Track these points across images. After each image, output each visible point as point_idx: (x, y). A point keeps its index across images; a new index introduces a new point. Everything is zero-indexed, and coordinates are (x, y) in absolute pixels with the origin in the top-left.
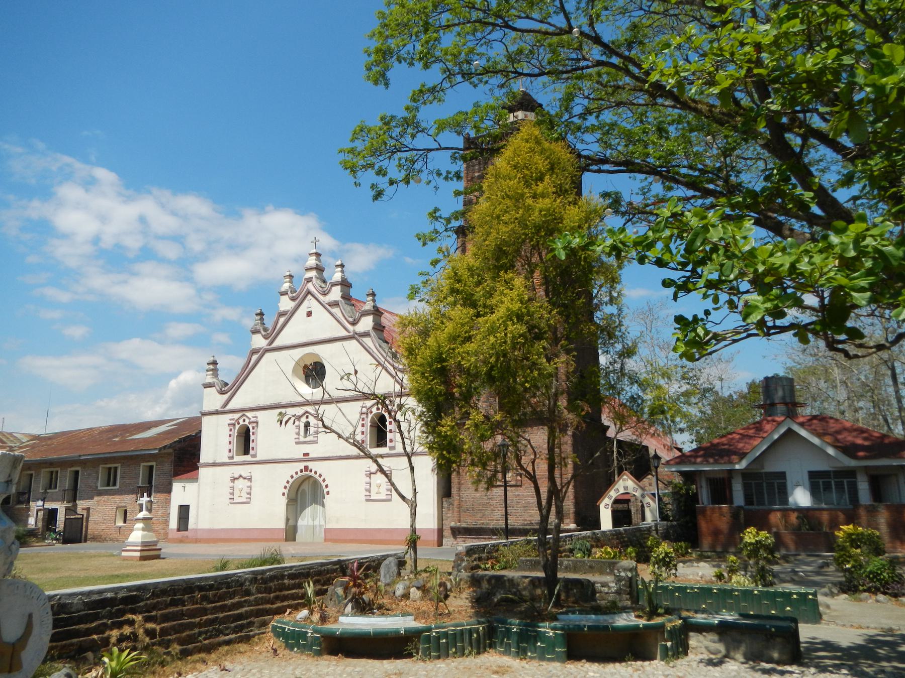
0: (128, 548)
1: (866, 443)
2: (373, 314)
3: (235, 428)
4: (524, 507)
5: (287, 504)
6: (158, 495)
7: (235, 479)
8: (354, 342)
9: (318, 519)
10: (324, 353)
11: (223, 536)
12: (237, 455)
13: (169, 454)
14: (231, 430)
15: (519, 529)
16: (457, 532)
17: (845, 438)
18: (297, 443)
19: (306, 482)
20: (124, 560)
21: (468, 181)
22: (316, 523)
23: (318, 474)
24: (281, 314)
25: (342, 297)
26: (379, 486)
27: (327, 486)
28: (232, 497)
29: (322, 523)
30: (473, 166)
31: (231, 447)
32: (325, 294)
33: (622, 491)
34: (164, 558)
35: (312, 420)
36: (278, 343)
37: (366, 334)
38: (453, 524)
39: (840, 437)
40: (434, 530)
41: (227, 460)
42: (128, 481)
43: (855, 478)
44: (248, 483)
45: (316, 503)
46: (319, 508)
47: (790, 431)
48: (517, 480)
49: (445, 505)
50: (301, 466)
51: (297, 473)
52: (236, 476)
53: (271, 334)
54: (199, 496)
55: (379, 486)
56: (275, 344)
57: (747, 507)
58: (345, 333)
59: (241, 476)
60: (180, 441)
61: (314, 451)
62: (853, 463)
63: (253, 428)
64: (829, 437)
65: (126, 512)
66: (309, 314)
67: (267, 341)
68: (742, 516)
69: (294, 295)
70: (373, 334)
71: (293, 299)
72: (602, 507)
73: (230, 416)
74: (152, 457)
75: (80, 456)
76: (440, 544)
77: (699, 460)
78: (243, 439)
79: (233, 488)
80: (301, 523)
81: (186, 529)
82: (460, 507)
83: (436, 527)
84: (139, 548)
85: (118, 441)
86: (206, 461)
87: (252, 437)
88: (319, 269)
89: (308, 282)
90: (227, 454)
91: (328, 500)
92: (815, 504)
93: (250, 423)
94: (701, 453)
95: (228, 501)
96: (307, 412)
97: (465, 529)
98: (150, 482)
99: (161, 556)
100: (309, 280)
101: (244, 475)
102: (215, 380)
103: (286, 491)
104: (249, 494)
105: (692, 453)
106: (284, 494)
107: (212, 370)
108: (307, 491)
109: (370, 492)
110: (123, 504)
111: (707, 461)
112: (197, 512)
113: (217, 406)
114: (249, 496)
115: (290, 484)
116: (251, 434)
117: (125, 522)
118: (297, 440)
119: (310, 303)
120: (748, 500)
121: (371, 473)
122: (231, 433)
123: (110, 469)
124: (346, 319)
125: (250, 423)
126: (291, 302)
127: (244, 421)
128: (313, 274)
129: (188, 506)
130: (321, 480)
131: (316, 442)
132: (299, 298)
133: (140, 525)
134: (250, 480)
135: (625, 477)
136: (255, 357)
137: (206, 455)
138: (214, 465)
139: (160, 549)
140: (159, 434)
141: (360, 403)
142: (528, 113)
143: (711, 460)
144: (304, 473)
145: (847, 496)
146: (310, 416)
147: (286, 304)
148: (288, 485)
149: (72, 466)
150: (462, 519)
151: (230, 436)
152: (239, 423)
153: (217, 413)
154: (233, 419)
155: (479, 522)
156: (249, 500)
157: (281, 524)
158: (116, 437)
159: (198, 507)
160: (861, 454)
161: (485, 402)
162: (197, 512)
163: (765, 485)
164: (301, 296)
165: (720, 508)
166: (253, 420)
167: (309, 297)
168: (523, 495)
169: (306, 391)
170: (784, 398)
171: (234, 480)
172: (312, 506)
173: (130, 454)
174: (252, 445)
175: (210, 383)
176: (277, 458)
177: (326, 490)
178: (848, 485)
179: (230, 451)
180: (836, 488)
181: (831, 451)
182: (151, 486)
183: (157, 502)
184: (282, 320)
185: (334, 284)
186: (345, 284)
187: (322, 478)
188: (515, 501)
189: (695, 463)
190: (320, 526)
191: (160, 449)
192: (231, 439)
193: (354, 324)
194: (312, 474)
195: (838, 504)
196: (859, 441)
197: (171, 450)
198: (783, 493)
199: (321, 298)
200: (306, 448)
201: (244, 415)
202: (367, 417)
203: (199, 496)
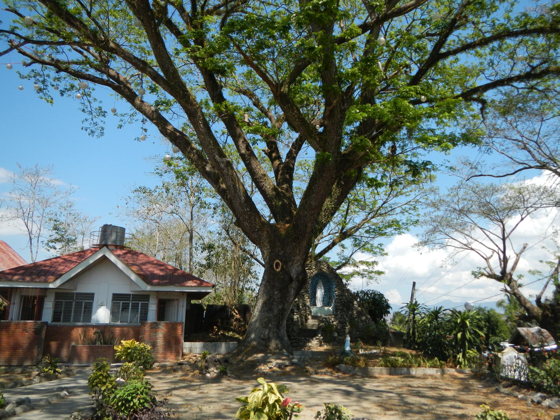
1: (161, 274)
17: (148, 268)
39: (144, 267)
43: (148, 301)
47: (104, 258)
57: (53, 323)
62: (149, 288)
64: (136, 267)
68: (44, 332)
77: (16, 277)
92: (112, 321)
94: (21, 272)
105: (13, 271)
111: (24, 279)
120: (56, 317)
143: (28, 279)
145: (139, 315)
160: (156, 281)
163: (74, 303)
165: (25, 324)
170: (115, 241)
178: (141, 306)
180: (132, 309)
181: (133, 277)
189: (11, 280)
195: (130, 322)
196: (157, 272)
198: (89, 310)
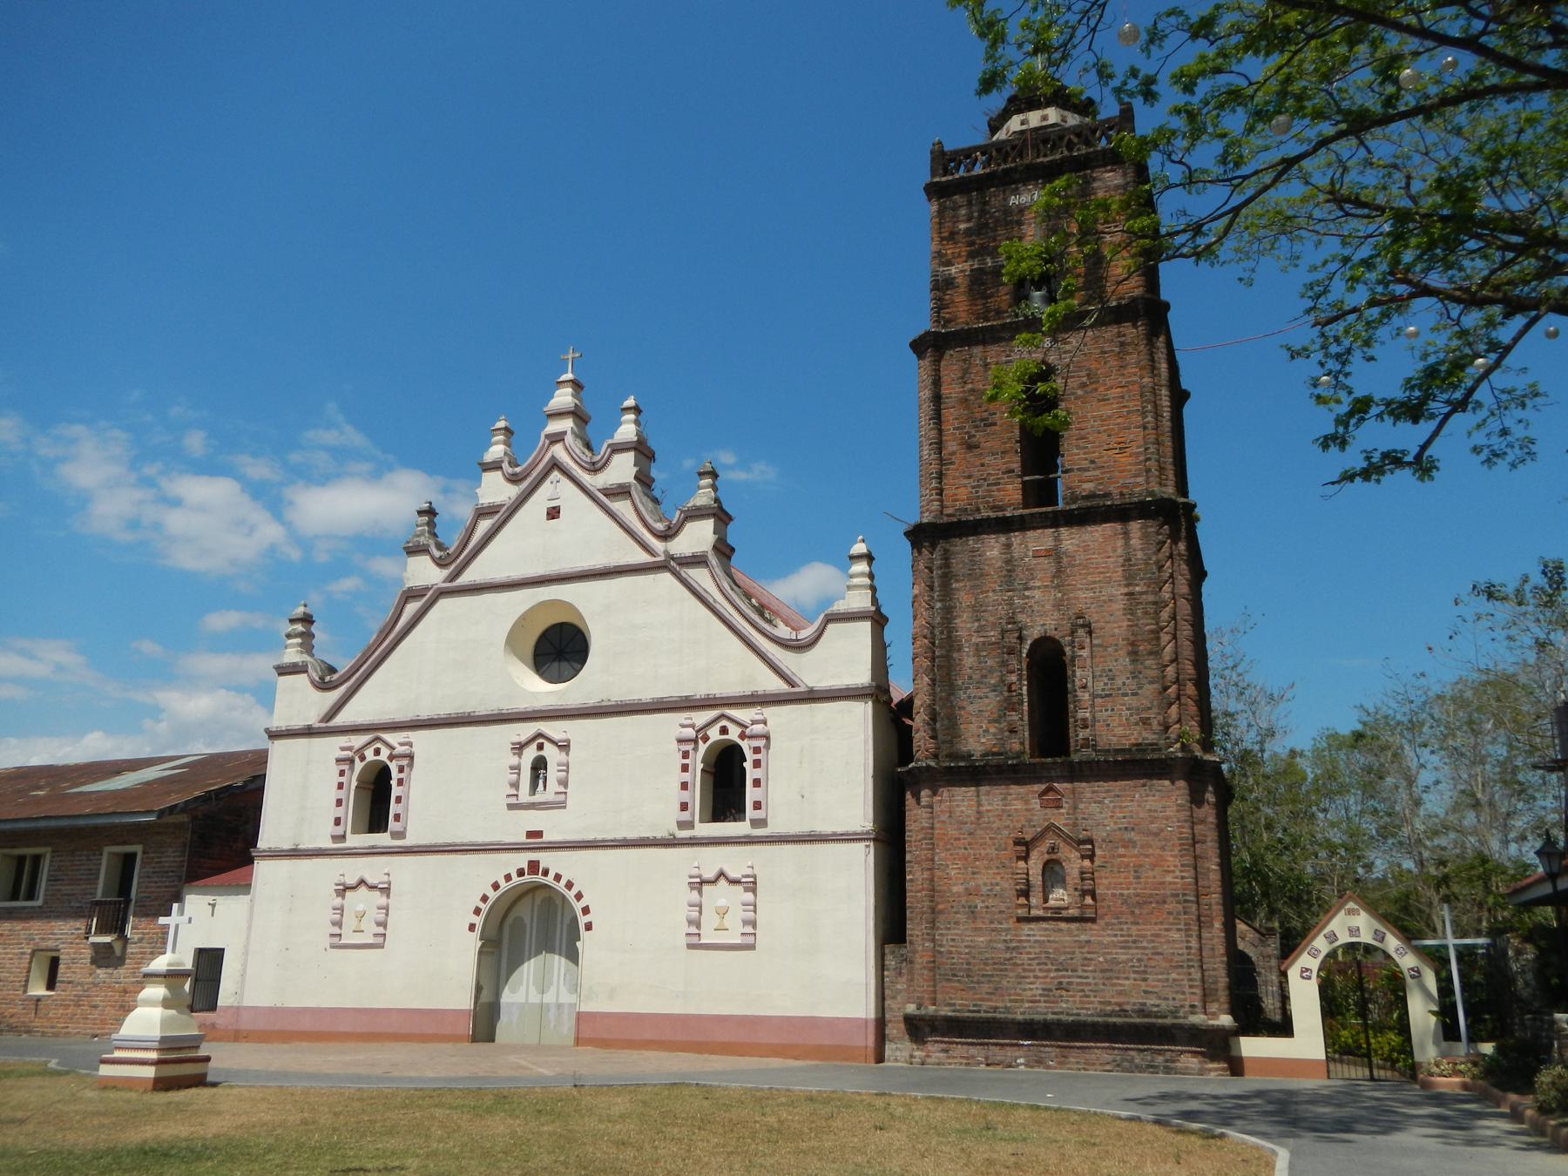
0: (118, 1054)
2: (714, 515)
3: (352, 769)
4: (1103, 971)
5: (480, 953)
6: (144, 922)
7: (347, 888)
8: (666, 577)
9: (553, 989)
10: (587, 602)
11: (307, 1024)
12: (354, 832)
13: (179, 827)
14: (342, 773)
15: (1094, 1025)
16: (918, 1029)
18: (511, 807)
19: (529, 898)
20: (105, 1088)
21: (942, 239)
22: (549, 998)
23: (563, 882)
24: (483, 513)
25: (636, 478)
26: (723, 912)
27: (586, 910)
28: (336, 930)
29: (567, 998)
30: (956, 208)
31: (340, 812)
32: (595, 469)
33: (1344, 938)
34: (214, 1085)
35: (550, 752)
36: (468, 577)
37: (698, 561)
38: (911, 1008)
40: (866, 1021)
41: (328, 844)
42: (67, 889)
44: (378, 898)
45: (551, 950)
46: (558, 962)
48: (1083, 907)
49: (891, 962)
50: (522, 860)
51: (508, 878)
52: (351, 880)
53: (455, 559)
54: (249, 928)
55: (723, 912)
56: (466, 578)
58: (642, 557)
59: (362, 882)
60: (207, 798)
61: (555, 826)
63: (401, 770)
65: (54, 963)
66: (554, 513)
67: (446, 572)
69: (518, 470)
70: (713, 560)
71: (514, 479)
72: (1293, 974)
73: (343, 740)
74: (137, 832)
76: (880, 1058)
78: (368, 796)
79: (341, 909)
80: (507, 997)
81: (212, 1007)
82: (933, 966)
83: (872, 1015)
84: (153, 1055)
85: (44, 797)
86: (273, 845)
87: (396, 791)
88: (578, 415)
89: (553, 443)
90: (330, 828)
93: (391, 758)
95: (327, 941)
96: (540, 735)
97: (948, 1020)
98: (123, 886)
99: (210, 1079)
100: (557, 438)
101: (370, 881)
102: (306, 658)
103: (479, 921)
104: (383, 924)
106: (472, 927)
107: (301, 635)
108: (527, 921)
109: (698, 926)
110: (51, 944)
112: (245, 965)
113: (312, 718)
114: (380, 930)
115: (490, 902)
116: (394, 783)
117: (51, 985)
118: (513, 800)
119: (557, 489)
121: (703, 882)
122: (342, 779)
123: (21, 860)
124: (646, 525)
125: (391, 758)
126: (509, 485)
127: (377, 752)
128: (567, 424)
129: (222, 950)
130: (571, 895)
131: (561, 805)
132: (528, 481)
133: (157, 991)
134: (386, 891)
135: (1351, 905)
136: (412, 608)
137: (273, 830)
138: (296, 853)
139: (207, 1059)
140: (148, 783)
141: (681, 717)
142: (1066, 113)
144: (527, 878)
146: (547, 745)
147: (495, 489)
148: (485, 907)
150: (939, 996)
151: (340, 786)
152: (363, 758)
153: (308, 732)
154: (350, 749)
155: (986, 1005)
156: (380, 940)
157: (463, 1000)
158: (39, 788)
159: (246, 953)
161: (996, 721)
162: (245, 965)
164: (535, 474)
166: (400, 750)
167: (556, 475)
168: (1100, 943)
169: (536, 689)
171: (344, 890)
172: (541, 958)
173: (81, 822)
174: (394, 808)
175: (295, 665)
176: (458, 841)
177: (583, 920)
179: (337, 822)
182: (128, 901)
183: (141, 940)
184: (484, 525)
185: (618, 449)
186: (642, 450)
187: (574, 891)
188: (1078, 956)
190: (559, 1006)
191: (161, 813)
192: (342, 794)
193: (666, 536)
194: (549, 880)
197: (184, 818)
199: (586, 478)
200: (534, 820)
201: (378, 739)
202: (696, 749)
203: (249, 928)
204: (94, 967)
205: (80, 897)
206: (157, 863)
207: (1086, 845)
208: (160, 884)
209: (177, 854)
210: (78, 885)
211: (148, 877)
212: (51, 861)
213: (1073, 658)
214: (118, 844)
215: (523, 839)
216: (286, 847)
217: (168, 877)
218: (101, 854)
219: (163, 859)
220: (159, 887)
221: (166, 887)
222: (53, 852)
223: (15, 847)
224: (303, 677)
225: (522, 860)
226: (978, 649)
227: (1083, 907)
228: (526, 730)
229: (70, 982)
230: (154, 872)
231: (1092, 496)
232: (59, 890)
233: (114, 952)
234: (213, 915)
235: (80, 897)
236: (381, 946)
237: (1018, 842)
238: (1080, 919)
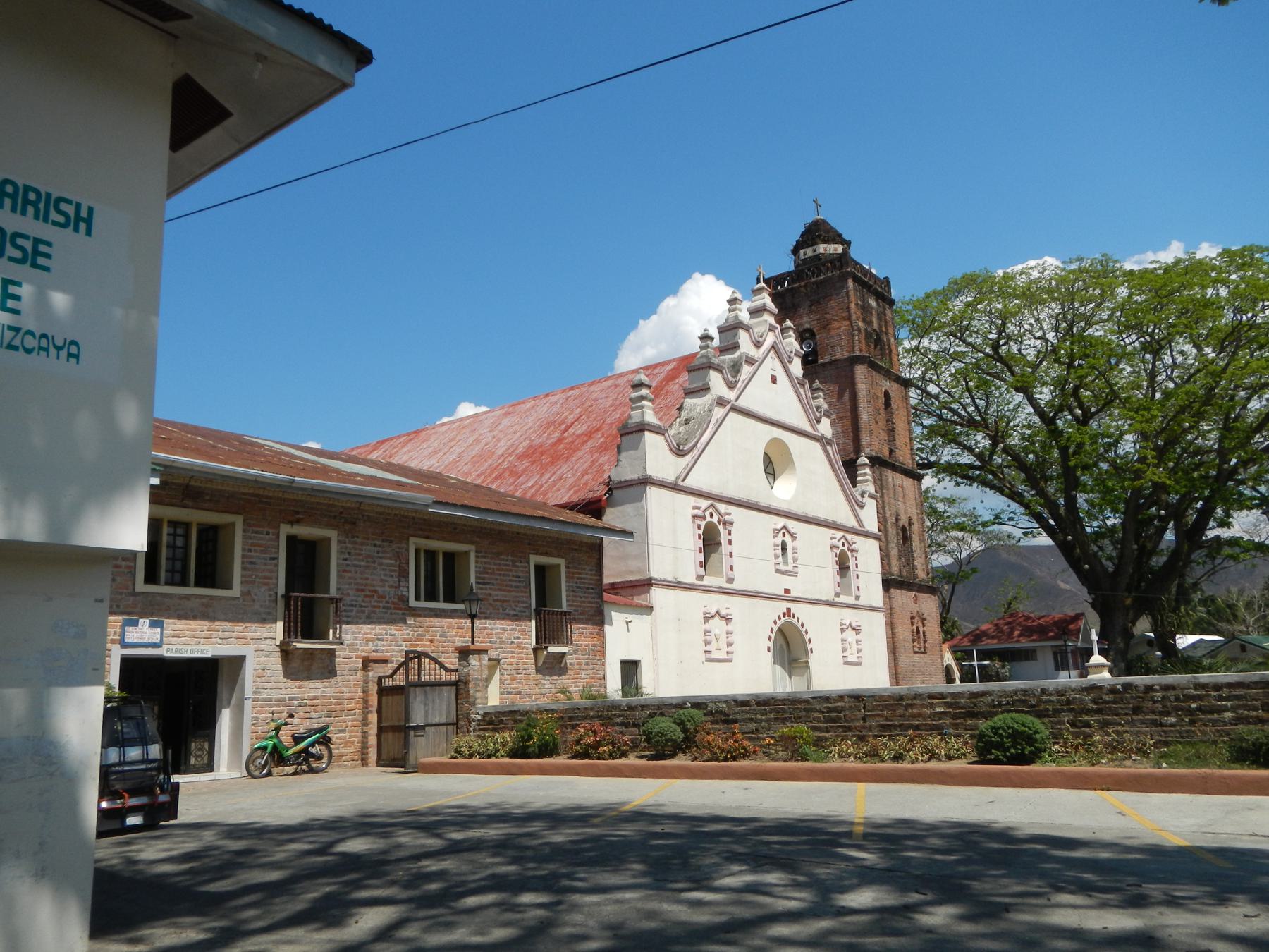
8: (817, 445)
14: (699, 527)
27: (810, 641)
35: (788, 539)
37: (829, 442)
50: (783, 606)
59: (718, 612)
73: (693, 500)
75: (437, 503)
91: (814, 660)
95: (703, 657)
103: (771, 644)
106: (769, 650)
113: (670, 477)
125: (719, 522)
127: (712, 516)
141: (830, 532)
146: (787, 534)
149: (298, 522)
175: (659, 427)
183: (576, 652)
200: (787, 582)
204: (540, 676)
205: (513, 604)
206: (578, 578)
207: (924, 620)
208: (583, 599)
209: (594, 572)
210: (509, 591)
211: (573, 591)
212: (477, 562)
213: (911, 538)
214: (542, 554)
215: (782, 593)
216: (670, 579)
217: (591, 593)
218: (528, 563)
219: (583, 576)
220: (584, 602)
221: (590, 602)
222: (476, 552)
223: (427, 538)
224: (663, 437)
225: (783, 606)
226: (891, 523)
227: (925, 647)
228: (780, 522)
229: (519, 693)
230: (577, 587)
231: (902, 463)
232: (490, 595)
233: (561, 662)
234: (628, 631)
235: (513, 604)
236: (730, 660)
237: (912, 618)
238: (924, 653)
